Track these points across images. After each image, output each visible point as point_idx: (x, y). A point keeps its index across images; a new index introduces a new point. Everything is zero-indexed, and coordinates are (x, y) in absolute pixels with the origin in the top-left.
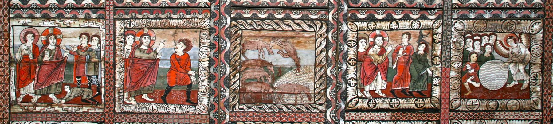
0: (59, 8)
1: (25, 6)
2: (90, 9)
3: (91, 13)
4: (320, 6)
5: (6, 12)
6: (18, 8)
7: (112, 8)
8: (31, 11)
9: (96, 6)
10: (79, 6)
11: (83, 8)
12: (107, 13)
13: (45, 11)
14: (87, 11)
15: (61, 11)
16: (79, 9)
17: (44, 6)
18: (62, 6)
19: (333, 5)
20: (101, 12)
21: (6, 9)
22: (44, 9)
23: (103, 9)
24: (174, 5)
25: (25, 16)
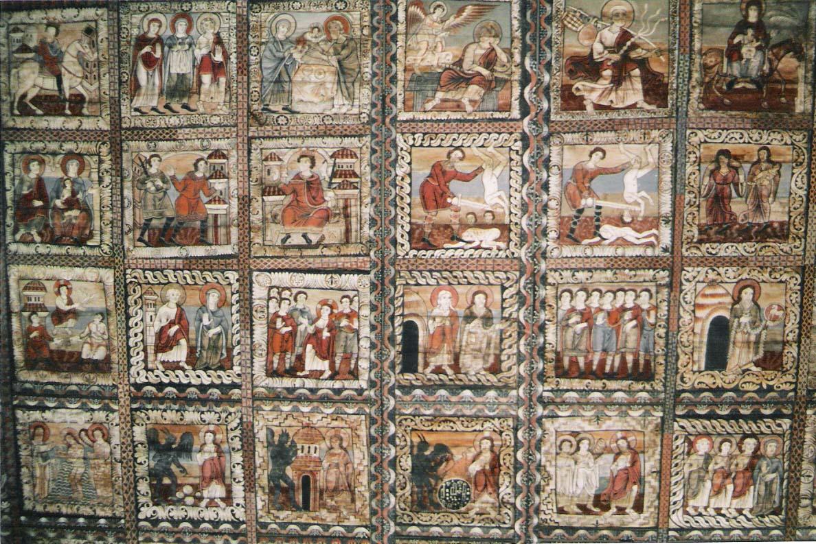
0: (194, 533)
1: (155, 529)
2: (229, 534)
3: (230, 539)
4: (505, 537)
5: (134, 535)
6: (147, 531)
7: (254, 534)
8: (161, 535)
9: (237, 531)
10: (216, 531)
11: (221, 533)
12: (249, 540)
13: (178, 535)
14: (226, 537)
15: (196, 535)
16: (216, 534)
17: (176, 529)
18: (196, 530)
19: (520, 537)
20: (241, 538)
21: (134, 531)
22: (177, 533)
23: (245, 535)
24: (327, 534)
25: (156, 540)
